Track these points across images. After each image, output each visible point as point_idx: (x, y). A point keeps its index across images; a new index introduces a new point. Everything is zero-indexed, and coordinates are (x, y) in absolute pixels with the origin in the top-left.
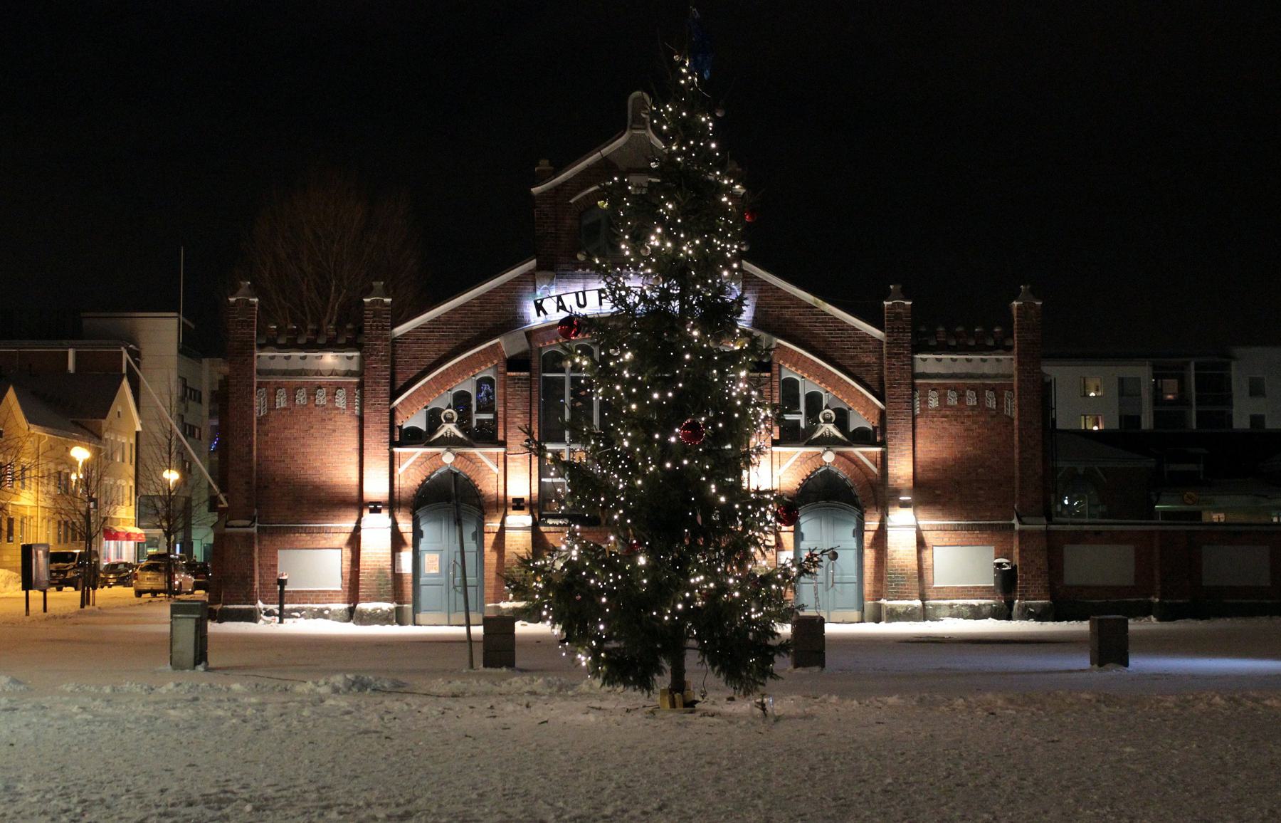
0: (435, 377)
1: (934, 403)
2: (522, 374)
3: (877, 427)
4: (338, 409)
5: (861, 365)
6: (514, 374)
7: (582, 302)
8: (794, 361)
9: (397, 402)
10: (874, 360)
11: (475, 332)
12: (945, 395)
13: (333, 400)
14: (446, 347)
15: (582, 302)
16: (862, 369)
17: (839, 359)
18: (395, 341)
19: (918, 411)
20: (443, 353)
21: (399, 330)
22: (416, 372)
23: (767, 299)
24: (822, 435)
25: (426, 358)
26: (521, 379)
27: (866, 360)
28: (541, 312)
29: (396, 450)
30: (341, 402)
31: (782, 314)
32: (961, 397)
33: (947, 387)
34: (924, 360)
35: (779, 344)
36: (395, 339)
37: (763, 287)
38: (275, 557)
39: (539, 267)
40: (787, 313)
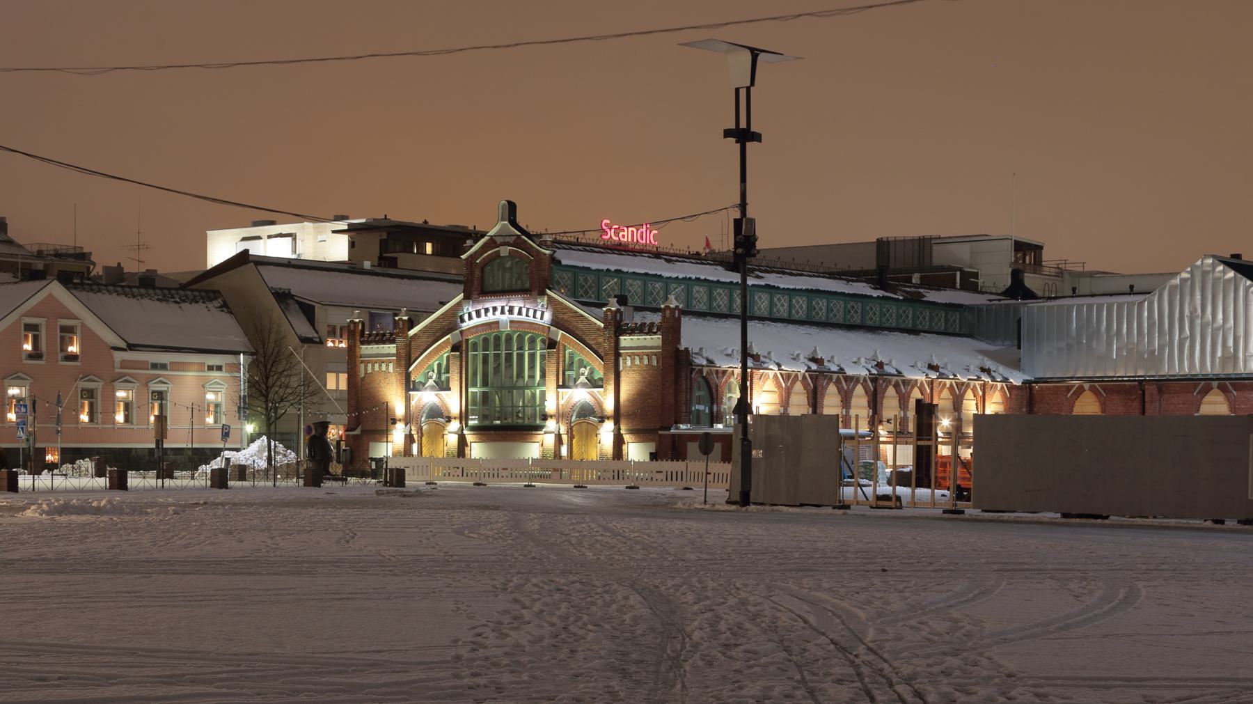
0: (426, 356)
1: (629, 363)
4: (390, 373)
5: (597, 343)
9: (411, 369)
12: (634, 359)
13: (387, 369)
14: (430, 340)
19: (621, 368)
21: (412, 332)
30: (391, 369)
32: (641, 359)
33: (634, 354)
34: (625, 339)
38: (368, 447)
40: (566, 317)
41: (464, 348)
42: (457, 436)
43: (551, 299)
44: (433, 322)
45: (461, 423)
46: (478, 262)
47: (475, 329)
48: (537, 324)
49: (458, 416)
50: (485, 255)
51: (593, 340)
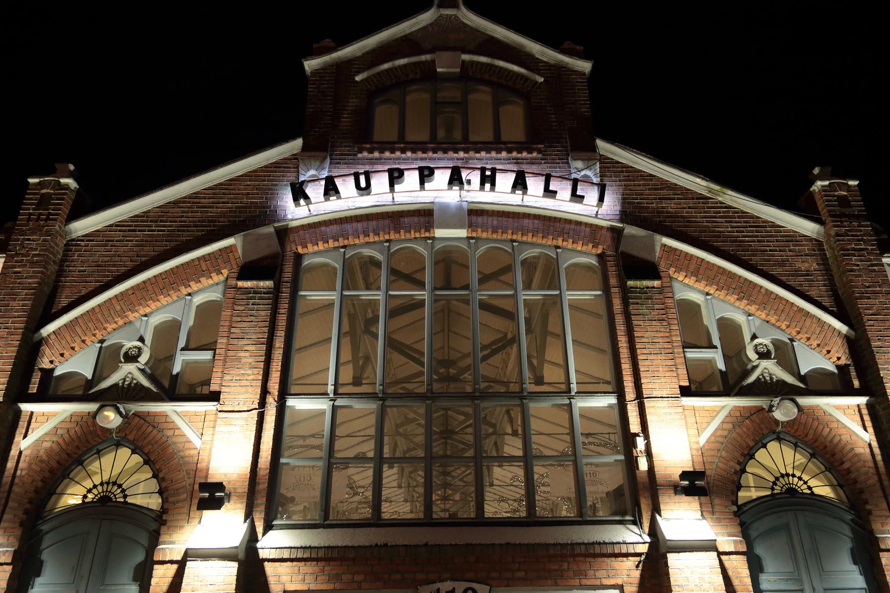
2: (262, 284)
3: (847, 366)
5: (797, 273)
6: (248, 284)
7: (363, 184)
8: (693, 267)
10: (815, 266)
11: (198, 231)
14: (150, 251)
15: (363, 184)
16: (802, 278)
17: (762, 265)
18: (72, 244)
20: (144, 259)
22: (93, 286)
23: (638, 188)
24: (758, 379)
25: (114, 266)
26: (260, 293)
27: (804, 267)
28: (302, 202)
29: (26, 407)
31: (663, 208)
35: (664, 246)
36: (73, 240)
37: (629, 174)
39: (305, 148)
40: (671, 206)
41: (288, 275)
42: (234, 566)
43: (609, 167)
44: (175, 203)
45: (249, 515)
46: (358, 78)
47: (335, 228)
48: (569, 222)
49: (244, 487)
50: (386, 66)
51: (782, 263)
